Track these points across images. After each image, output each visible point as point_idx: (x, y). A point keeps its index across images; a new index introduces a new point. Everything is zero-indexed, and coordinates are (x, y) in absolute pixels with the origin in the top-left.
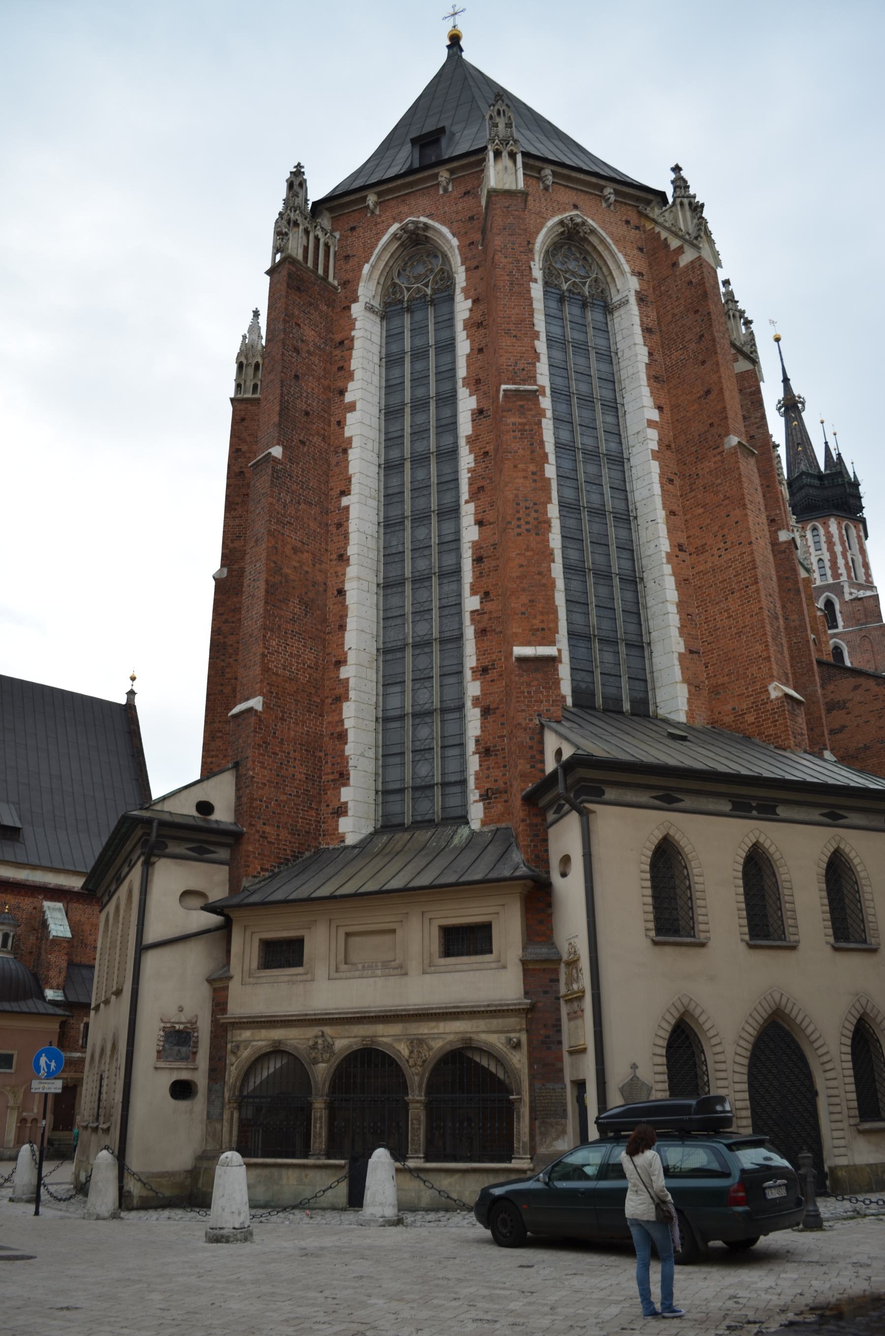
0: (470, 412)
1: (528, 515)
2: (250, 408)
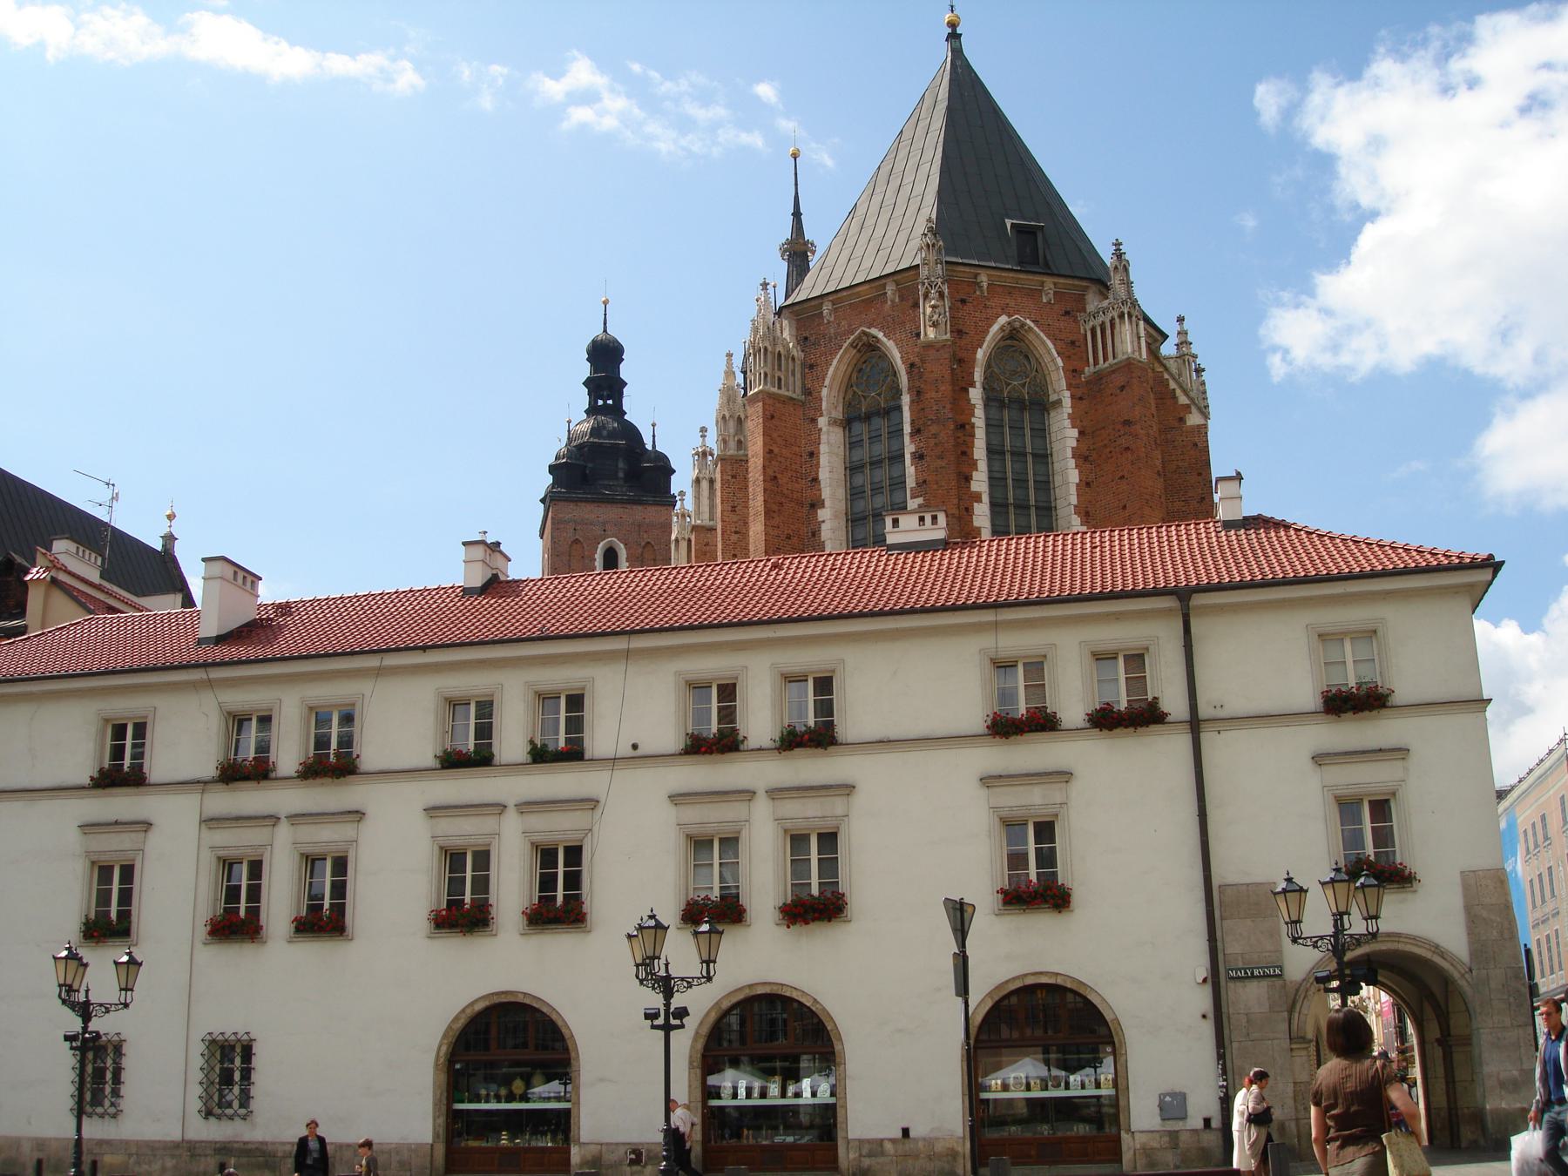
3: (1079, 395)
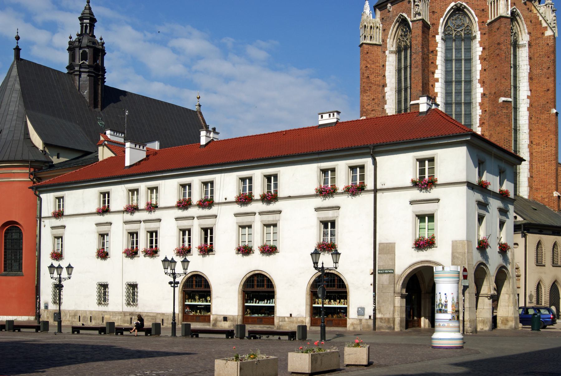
0: (480, 94)
1: (507, 144)
2: (370, 47)
3: (484, 32)
